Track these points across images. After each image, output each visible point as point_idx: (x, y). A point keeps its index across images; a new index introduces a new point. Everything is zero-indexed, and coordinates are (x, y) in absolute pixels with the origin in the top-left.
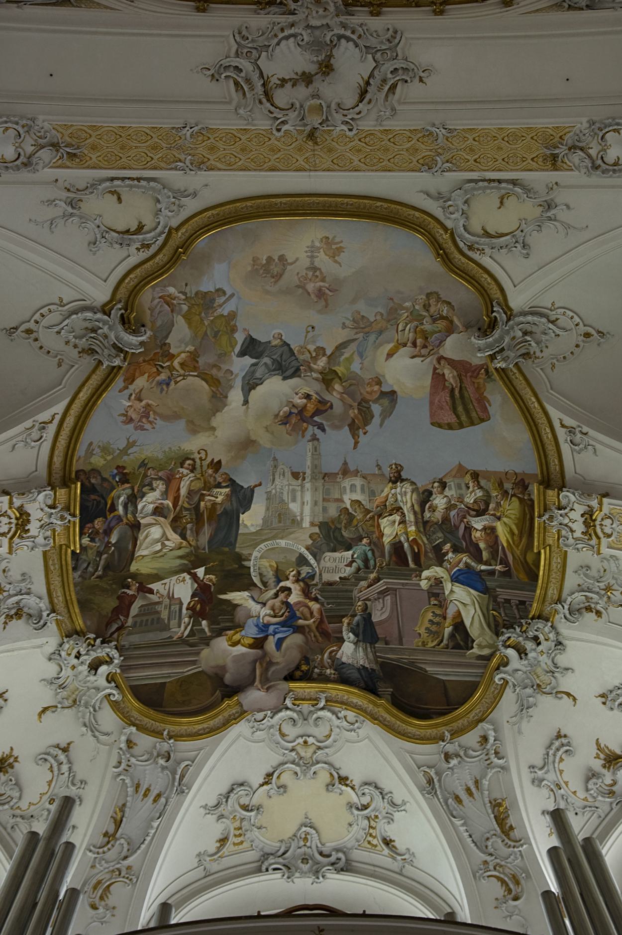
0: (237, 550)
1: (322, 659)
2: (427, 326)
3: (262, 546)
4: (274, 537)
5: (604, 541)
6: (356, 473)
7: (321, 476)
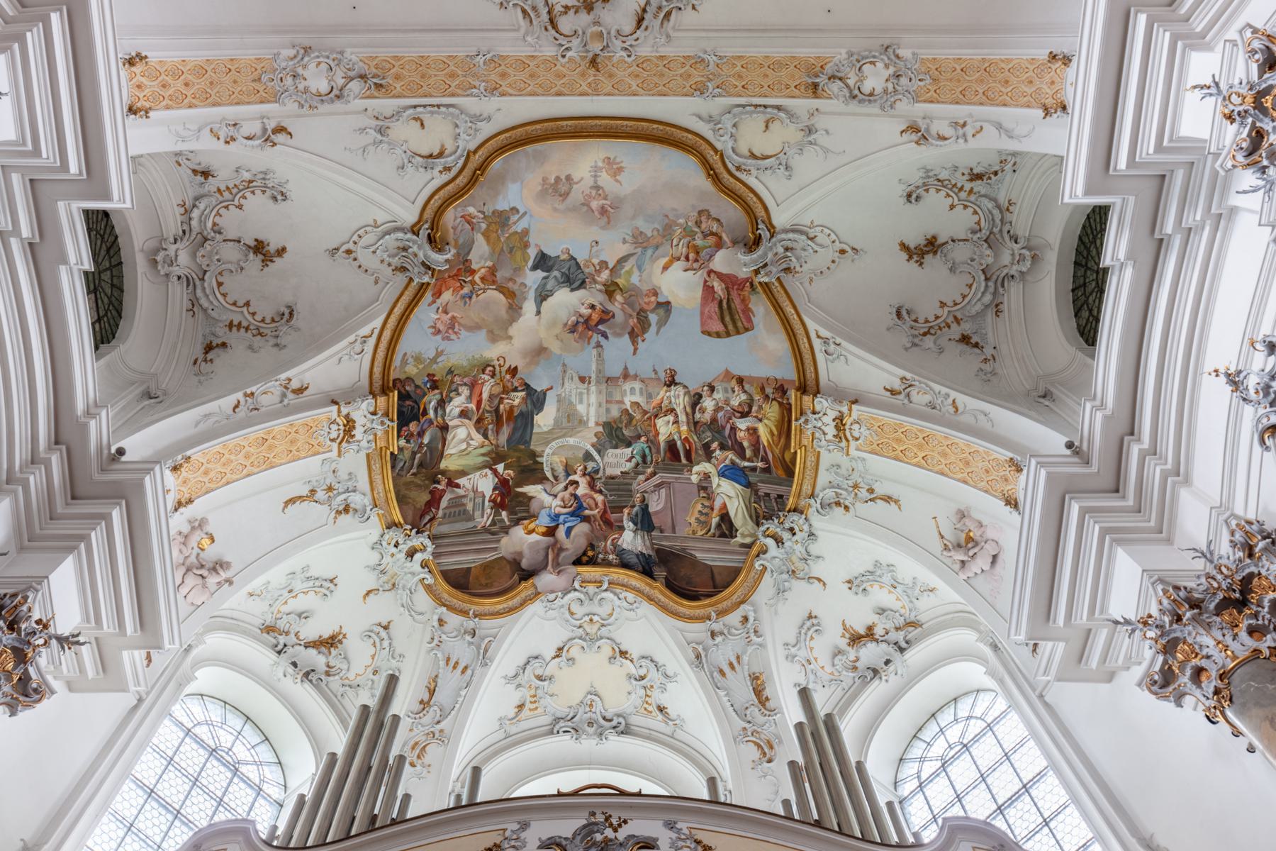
0: (532, 447)
1: (605, 546)
3: (553, 443)
4: (564, 436)
5: (853, 443)
6: (636, 377)
7: (605, 380)
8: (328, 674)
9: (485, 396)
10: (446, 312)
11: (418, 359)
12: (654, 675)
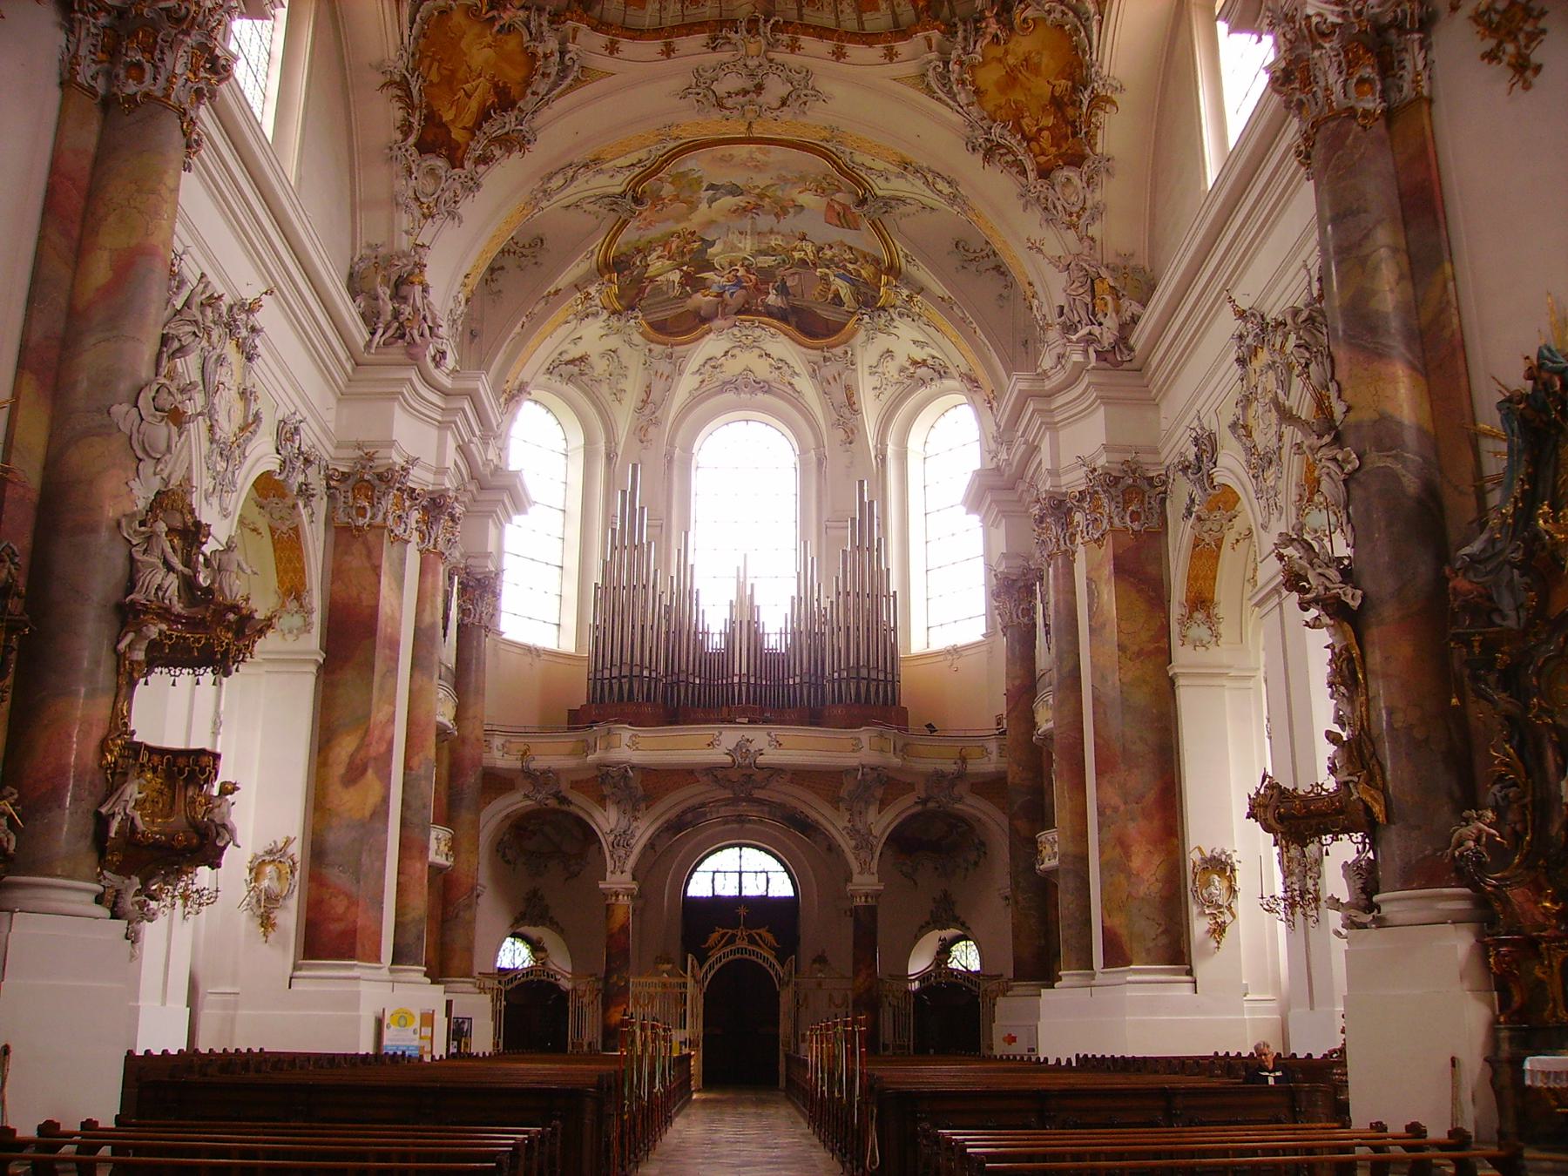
2: (825, 185)
6: (778, 233)
8: (581, 374)
9: (674, 246)
10: (645, 219)
11: (627, 243)
12: (785, 367)
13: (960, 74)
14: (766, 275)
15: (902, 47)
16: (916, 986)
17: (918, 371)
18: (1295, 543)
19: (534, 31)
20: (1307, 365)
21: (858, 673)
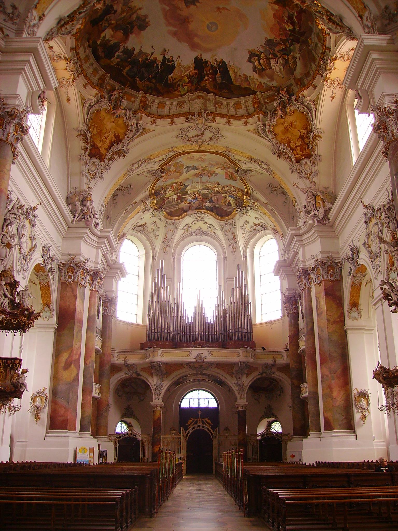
6: (209, 182)
8: (144, 230)
11: (159, 186)
12: (212, 227)
13: (269, 129)
14: (206, 196)
15: (250, 120)
16: (260, 438)
17: (257, 227)
18: (387, 284)
19: (128, 117)
20: (389, 223)
21: (238, 330)
